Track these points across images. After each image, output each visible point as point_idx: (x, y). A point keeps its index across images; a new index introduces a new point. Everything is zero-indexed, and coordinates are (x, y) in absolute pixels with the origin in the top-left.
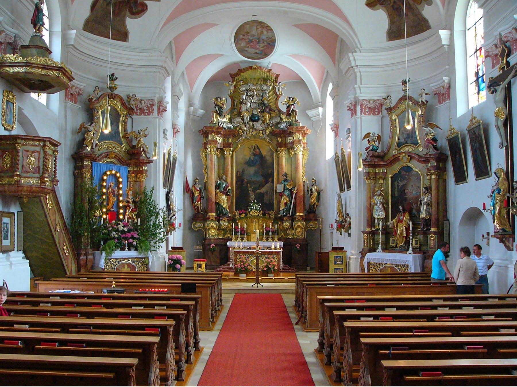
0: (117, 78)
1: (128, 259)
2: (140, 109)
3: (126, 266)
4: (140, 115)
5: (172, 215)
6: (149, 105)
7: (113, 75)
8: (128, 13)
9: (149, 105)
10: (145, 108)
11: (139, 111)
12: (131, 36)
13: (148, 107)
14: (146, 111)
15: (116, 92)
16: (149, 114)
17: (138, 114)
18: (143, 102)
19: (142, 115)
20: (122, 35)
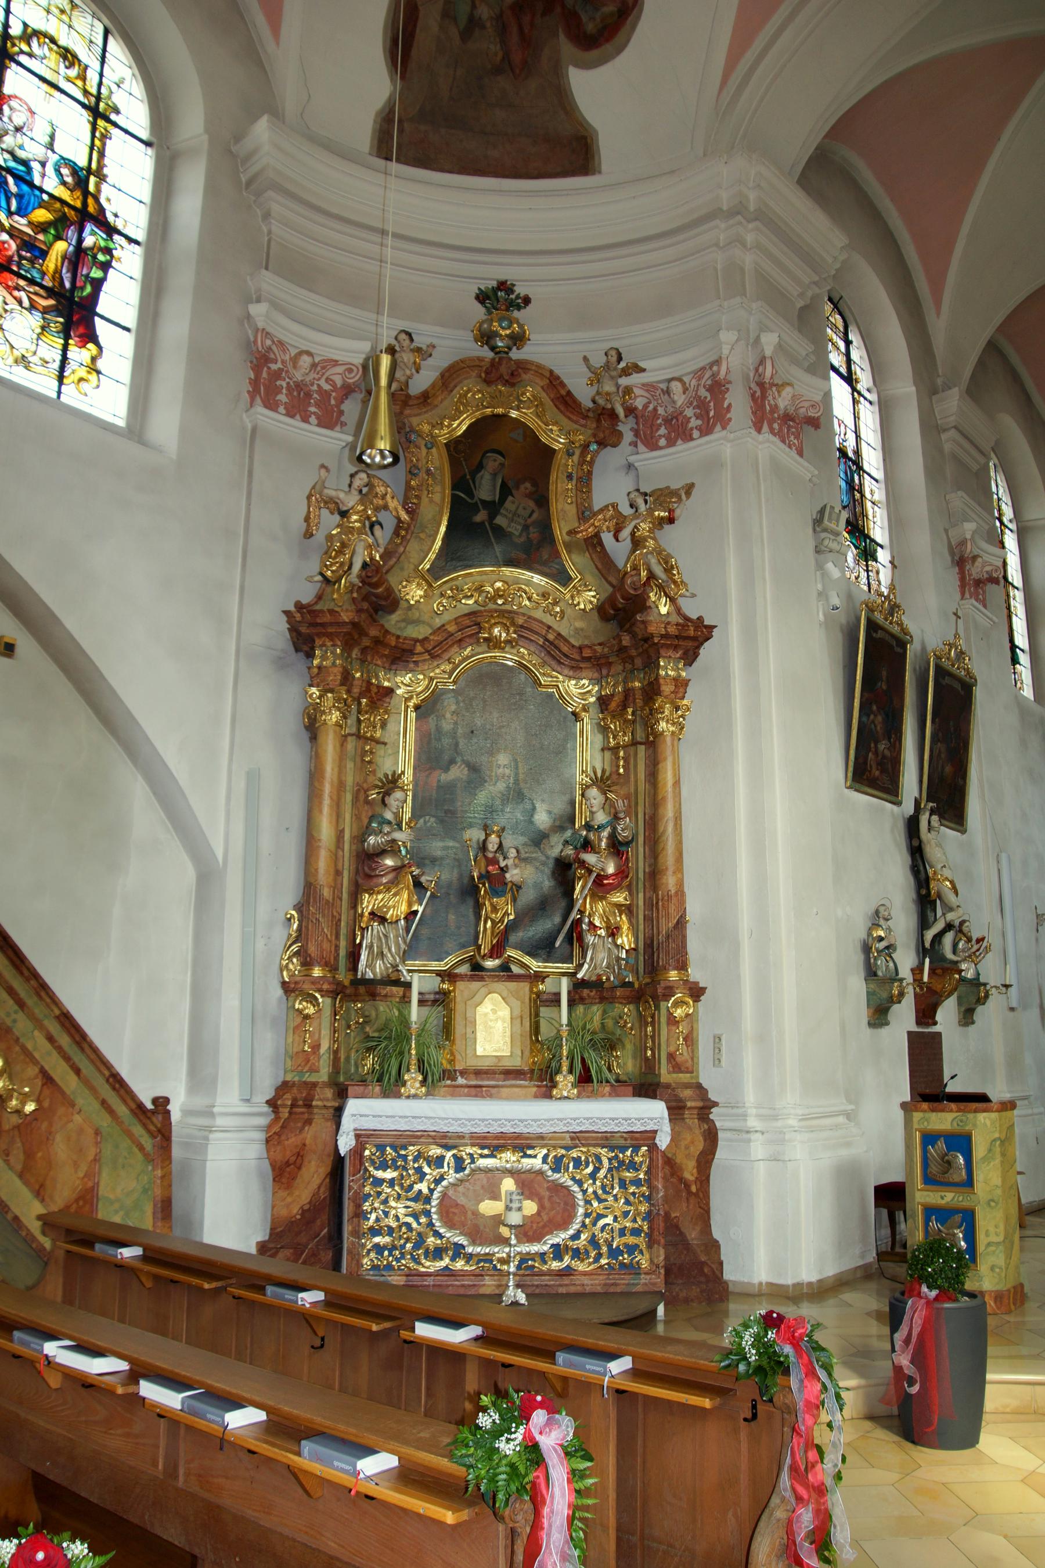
0: (527, 301)
1: (522, 1144)
2: (667, 421)
3: (508, 1184)
4: (671, 443)
5: (939, 926)
6: (703, 393)
7: (504, 286)
8: (566, 47)
9: (703, 393)
10: (689, 412)
11: (663, 431)
12: (609, 148)
13: (702, 405)
14: (694, 423)
15: (515, 354)
16: (706, 430)
17: (663, 442)
18: (676, 387)
19: (680, 446)
20: (573, 153)
